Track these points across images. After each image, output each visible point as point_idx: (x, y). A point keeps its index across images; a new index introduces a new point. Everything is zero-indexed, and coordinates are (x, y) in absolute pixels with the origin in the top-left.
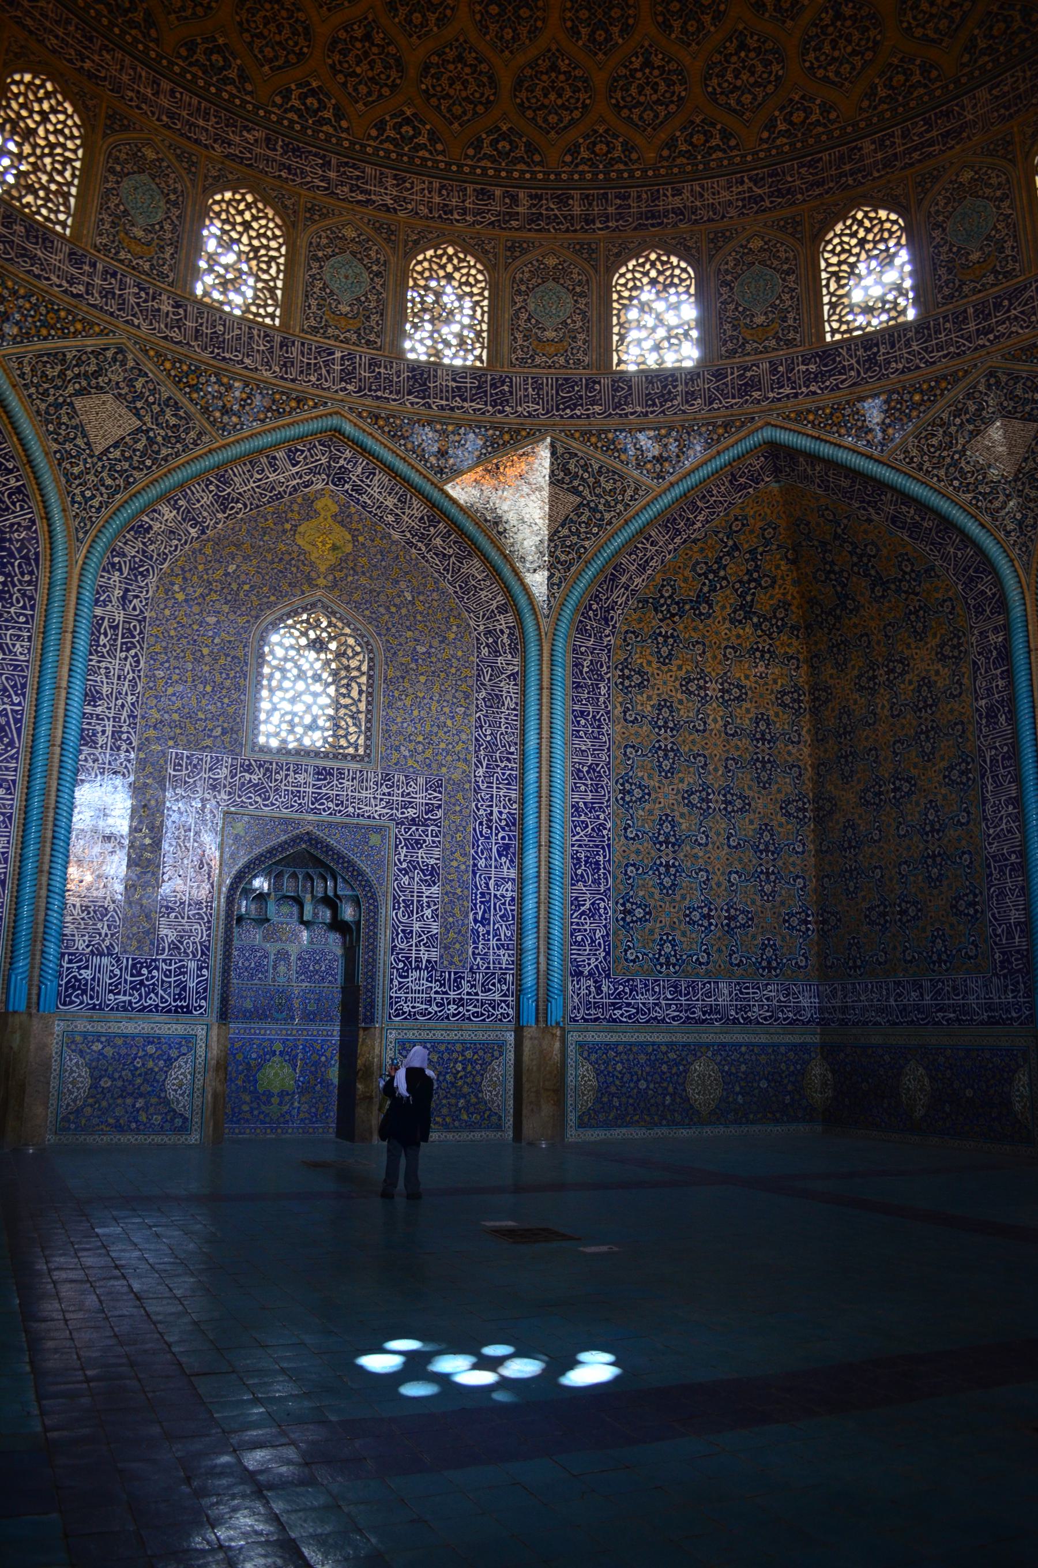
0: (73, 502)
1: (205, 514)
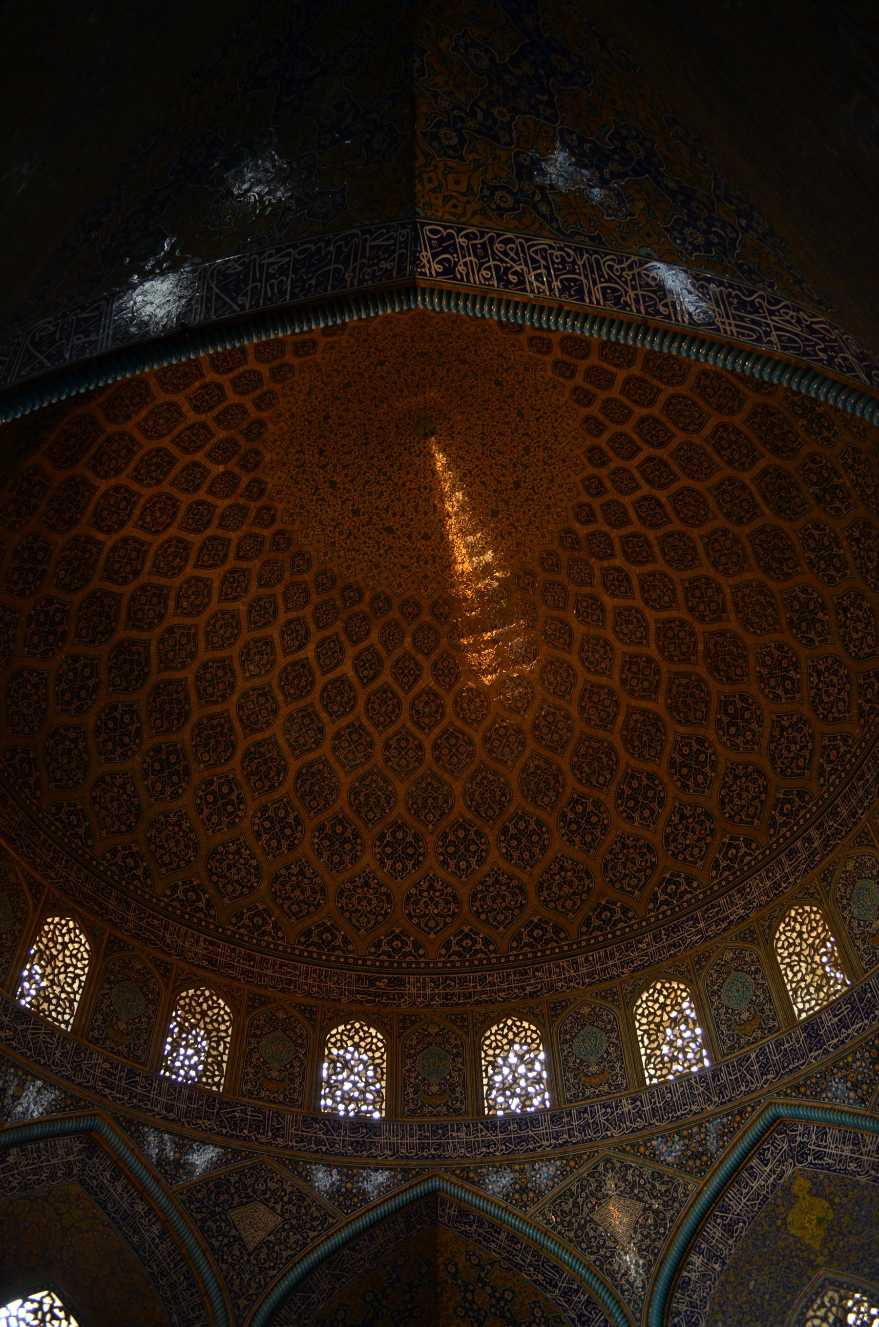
0: (623, 1292)
1: (721, 1246)
